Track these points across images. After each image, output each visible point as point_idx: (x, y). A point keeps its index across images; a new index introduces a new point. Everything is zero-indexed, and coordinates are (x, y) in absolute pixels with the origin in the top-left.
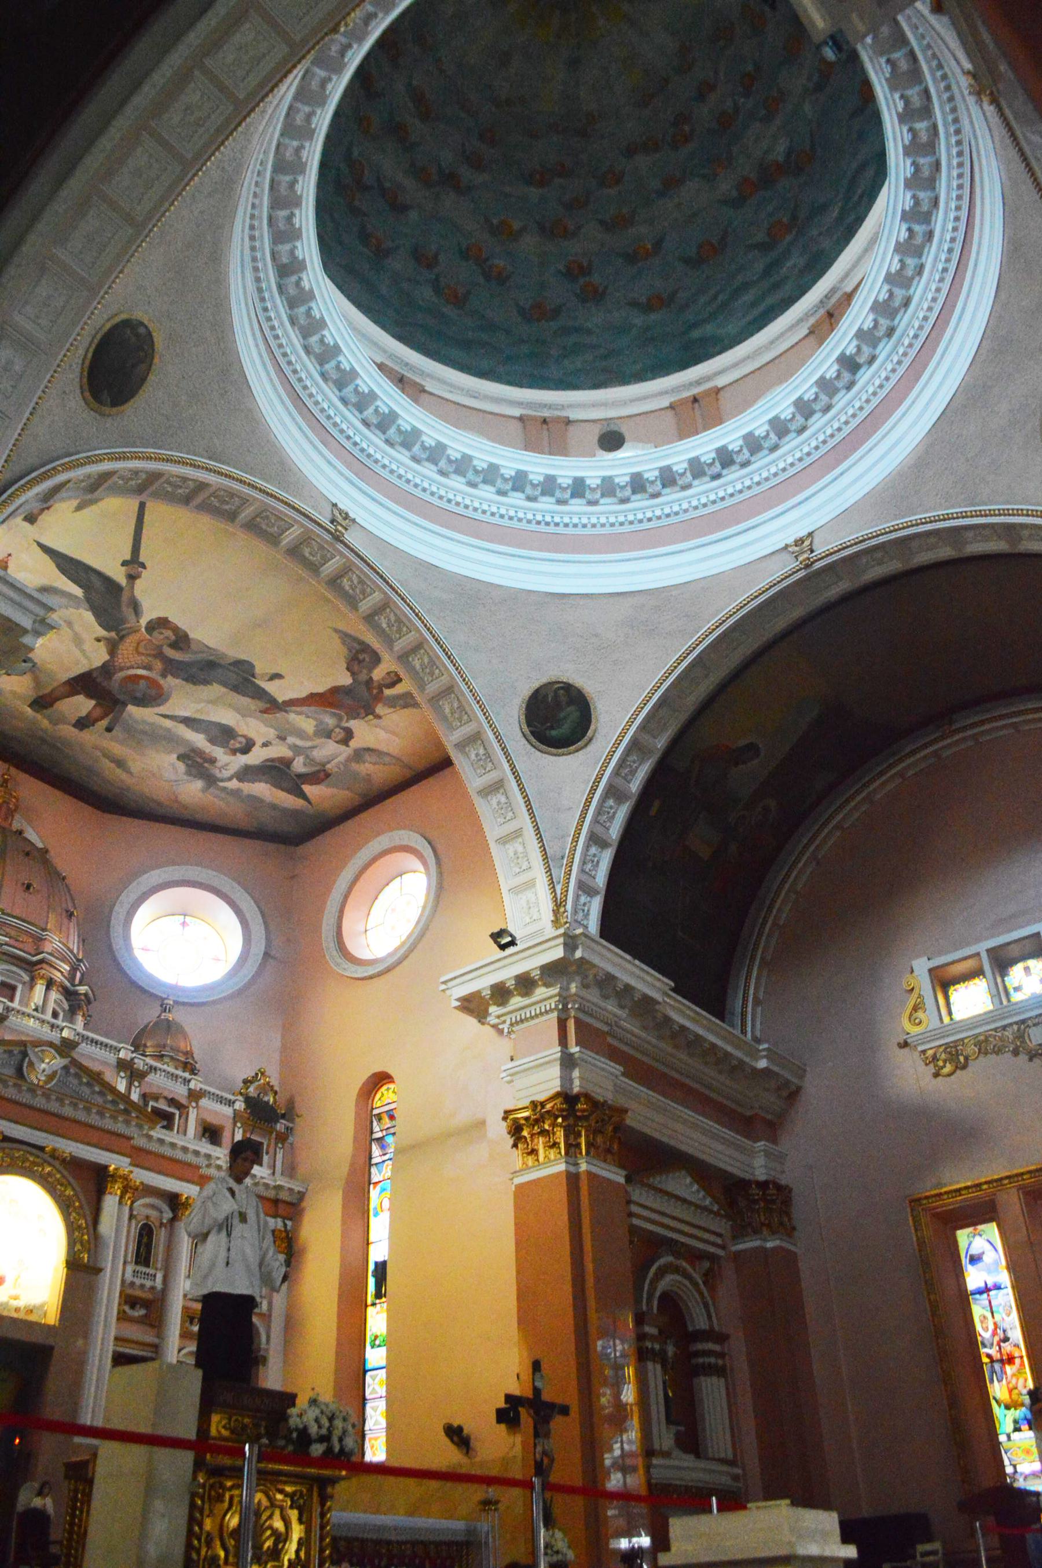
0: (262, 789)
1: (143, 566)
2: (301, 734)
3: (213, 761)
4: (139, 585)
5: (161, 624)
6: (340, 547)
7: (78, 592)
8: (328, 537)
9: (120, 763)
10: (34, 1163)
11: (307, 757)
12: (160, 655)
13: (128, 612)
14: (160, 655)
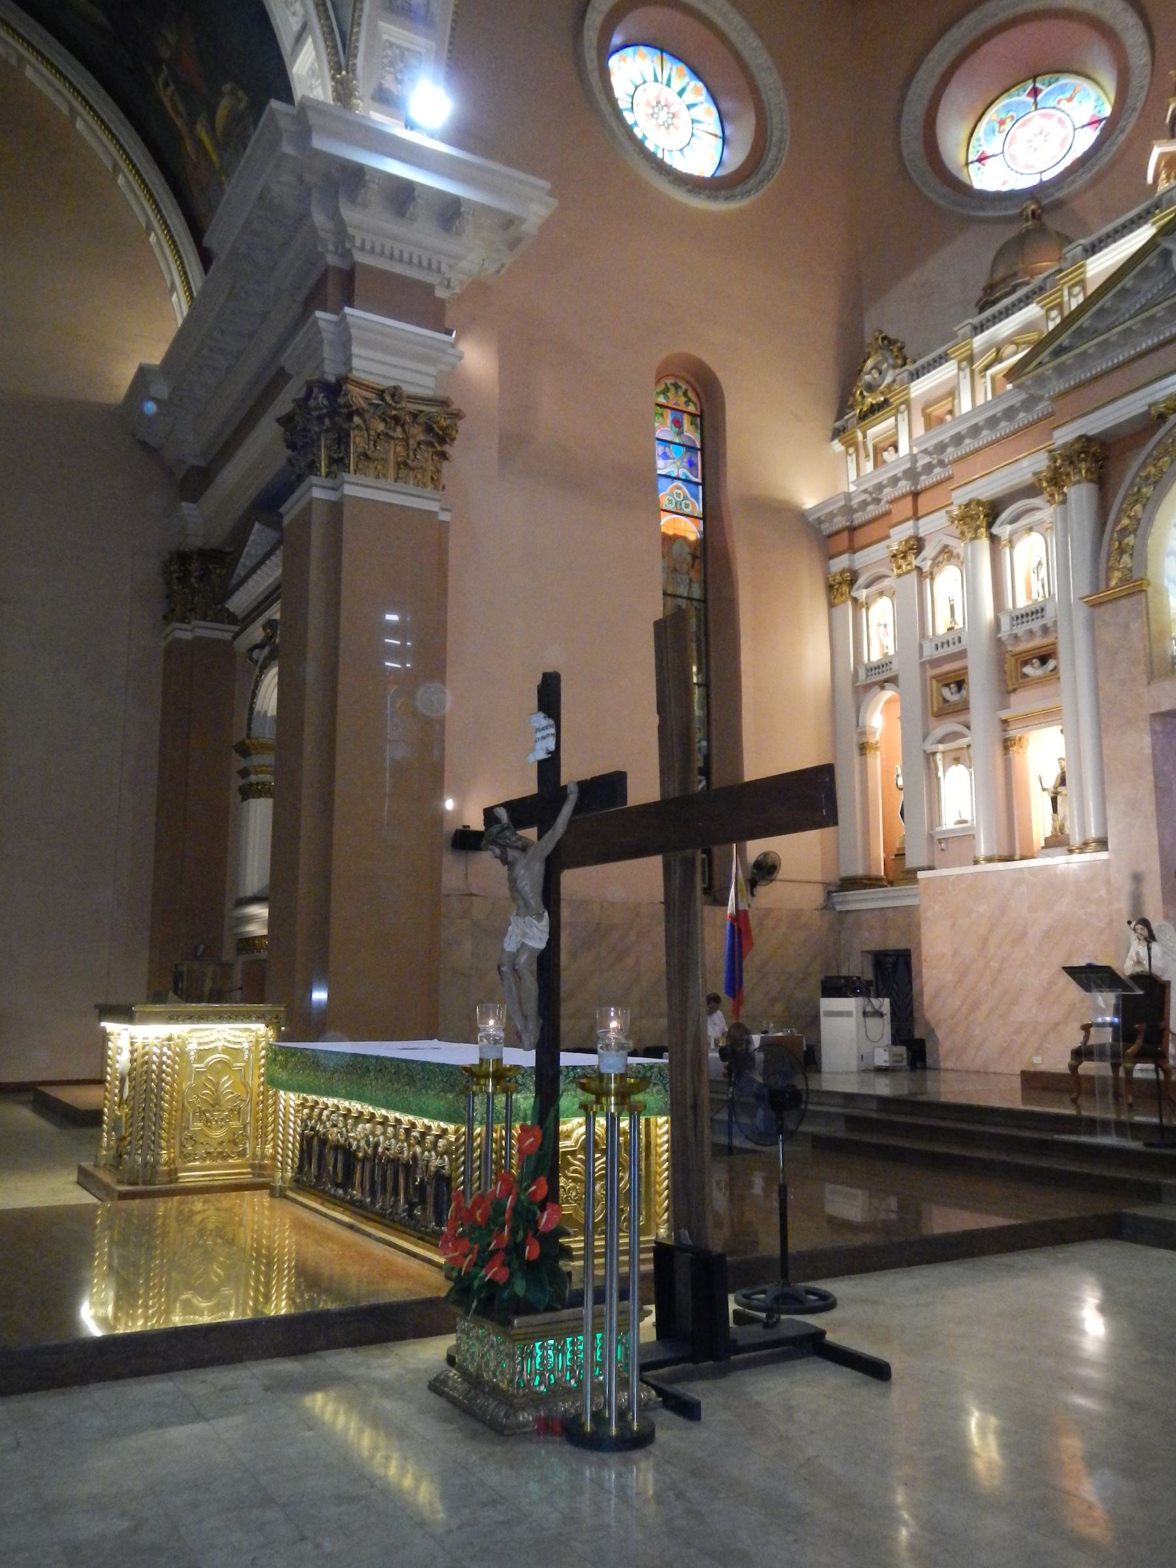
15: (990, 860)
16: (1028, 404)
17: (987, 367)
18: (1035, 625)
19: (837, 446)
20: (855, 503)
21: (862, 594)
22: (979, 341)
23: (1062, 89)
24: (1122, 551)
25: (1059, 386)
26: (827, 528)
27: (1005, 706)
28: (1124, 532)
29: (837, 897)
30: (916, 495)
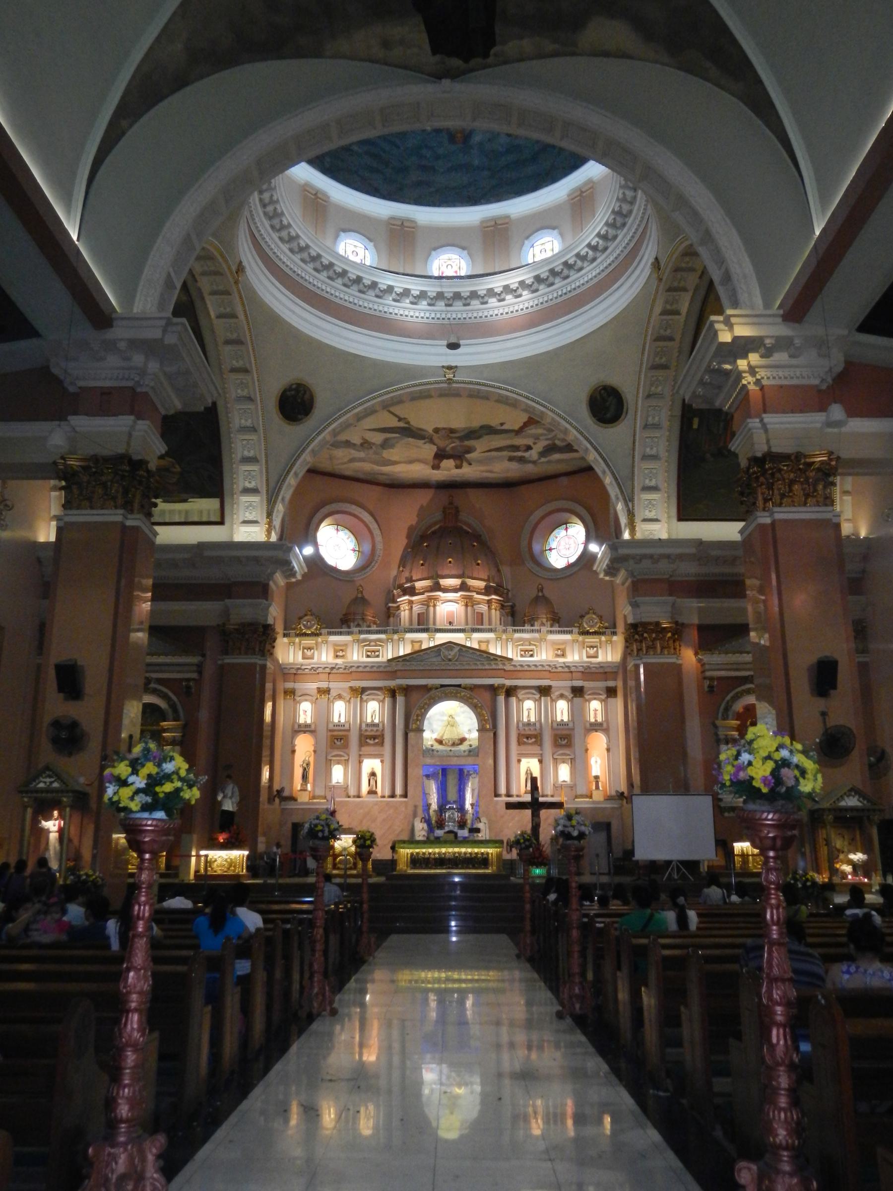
0: (557, 456)
1: (405, 418)
2: (542, 435)
3: (524, 457)
4: (412, 423)
5: (436, 430)
6: (454, 385)
7: (397, 435)
8: (445, 385)
9: (491, 472)
10: (457, 693)
11: (559, 439)
12: (451, 438)
13: (420, 432)
14: (451, 438)
15: (354, 797)
16: (385, 667)
17: (365, 646)
18: (375, 729)
19: (286, 640)
20: (303, 667)
21: (298, 699)
22: (362, 636)
23: (346, 533)
24: (417, 720)
25: (399, 668)
26: (286, 671)
27: (360, 750)
28: (418, 716)
29: (283, 803)
30: (329, 673)
